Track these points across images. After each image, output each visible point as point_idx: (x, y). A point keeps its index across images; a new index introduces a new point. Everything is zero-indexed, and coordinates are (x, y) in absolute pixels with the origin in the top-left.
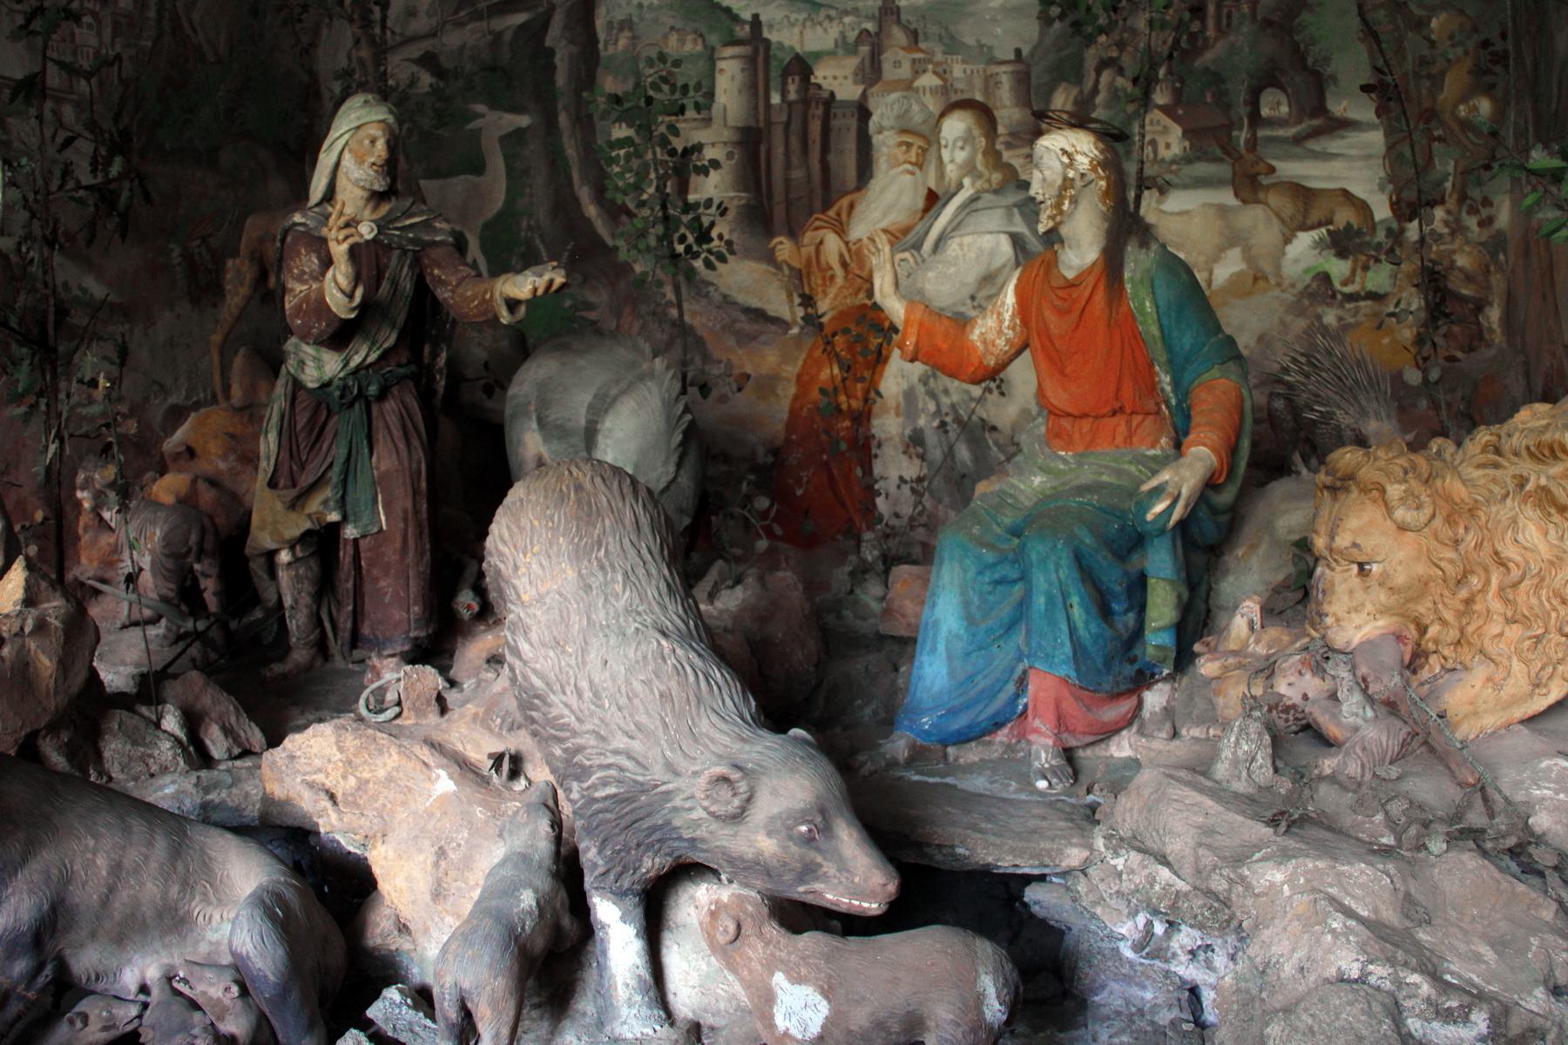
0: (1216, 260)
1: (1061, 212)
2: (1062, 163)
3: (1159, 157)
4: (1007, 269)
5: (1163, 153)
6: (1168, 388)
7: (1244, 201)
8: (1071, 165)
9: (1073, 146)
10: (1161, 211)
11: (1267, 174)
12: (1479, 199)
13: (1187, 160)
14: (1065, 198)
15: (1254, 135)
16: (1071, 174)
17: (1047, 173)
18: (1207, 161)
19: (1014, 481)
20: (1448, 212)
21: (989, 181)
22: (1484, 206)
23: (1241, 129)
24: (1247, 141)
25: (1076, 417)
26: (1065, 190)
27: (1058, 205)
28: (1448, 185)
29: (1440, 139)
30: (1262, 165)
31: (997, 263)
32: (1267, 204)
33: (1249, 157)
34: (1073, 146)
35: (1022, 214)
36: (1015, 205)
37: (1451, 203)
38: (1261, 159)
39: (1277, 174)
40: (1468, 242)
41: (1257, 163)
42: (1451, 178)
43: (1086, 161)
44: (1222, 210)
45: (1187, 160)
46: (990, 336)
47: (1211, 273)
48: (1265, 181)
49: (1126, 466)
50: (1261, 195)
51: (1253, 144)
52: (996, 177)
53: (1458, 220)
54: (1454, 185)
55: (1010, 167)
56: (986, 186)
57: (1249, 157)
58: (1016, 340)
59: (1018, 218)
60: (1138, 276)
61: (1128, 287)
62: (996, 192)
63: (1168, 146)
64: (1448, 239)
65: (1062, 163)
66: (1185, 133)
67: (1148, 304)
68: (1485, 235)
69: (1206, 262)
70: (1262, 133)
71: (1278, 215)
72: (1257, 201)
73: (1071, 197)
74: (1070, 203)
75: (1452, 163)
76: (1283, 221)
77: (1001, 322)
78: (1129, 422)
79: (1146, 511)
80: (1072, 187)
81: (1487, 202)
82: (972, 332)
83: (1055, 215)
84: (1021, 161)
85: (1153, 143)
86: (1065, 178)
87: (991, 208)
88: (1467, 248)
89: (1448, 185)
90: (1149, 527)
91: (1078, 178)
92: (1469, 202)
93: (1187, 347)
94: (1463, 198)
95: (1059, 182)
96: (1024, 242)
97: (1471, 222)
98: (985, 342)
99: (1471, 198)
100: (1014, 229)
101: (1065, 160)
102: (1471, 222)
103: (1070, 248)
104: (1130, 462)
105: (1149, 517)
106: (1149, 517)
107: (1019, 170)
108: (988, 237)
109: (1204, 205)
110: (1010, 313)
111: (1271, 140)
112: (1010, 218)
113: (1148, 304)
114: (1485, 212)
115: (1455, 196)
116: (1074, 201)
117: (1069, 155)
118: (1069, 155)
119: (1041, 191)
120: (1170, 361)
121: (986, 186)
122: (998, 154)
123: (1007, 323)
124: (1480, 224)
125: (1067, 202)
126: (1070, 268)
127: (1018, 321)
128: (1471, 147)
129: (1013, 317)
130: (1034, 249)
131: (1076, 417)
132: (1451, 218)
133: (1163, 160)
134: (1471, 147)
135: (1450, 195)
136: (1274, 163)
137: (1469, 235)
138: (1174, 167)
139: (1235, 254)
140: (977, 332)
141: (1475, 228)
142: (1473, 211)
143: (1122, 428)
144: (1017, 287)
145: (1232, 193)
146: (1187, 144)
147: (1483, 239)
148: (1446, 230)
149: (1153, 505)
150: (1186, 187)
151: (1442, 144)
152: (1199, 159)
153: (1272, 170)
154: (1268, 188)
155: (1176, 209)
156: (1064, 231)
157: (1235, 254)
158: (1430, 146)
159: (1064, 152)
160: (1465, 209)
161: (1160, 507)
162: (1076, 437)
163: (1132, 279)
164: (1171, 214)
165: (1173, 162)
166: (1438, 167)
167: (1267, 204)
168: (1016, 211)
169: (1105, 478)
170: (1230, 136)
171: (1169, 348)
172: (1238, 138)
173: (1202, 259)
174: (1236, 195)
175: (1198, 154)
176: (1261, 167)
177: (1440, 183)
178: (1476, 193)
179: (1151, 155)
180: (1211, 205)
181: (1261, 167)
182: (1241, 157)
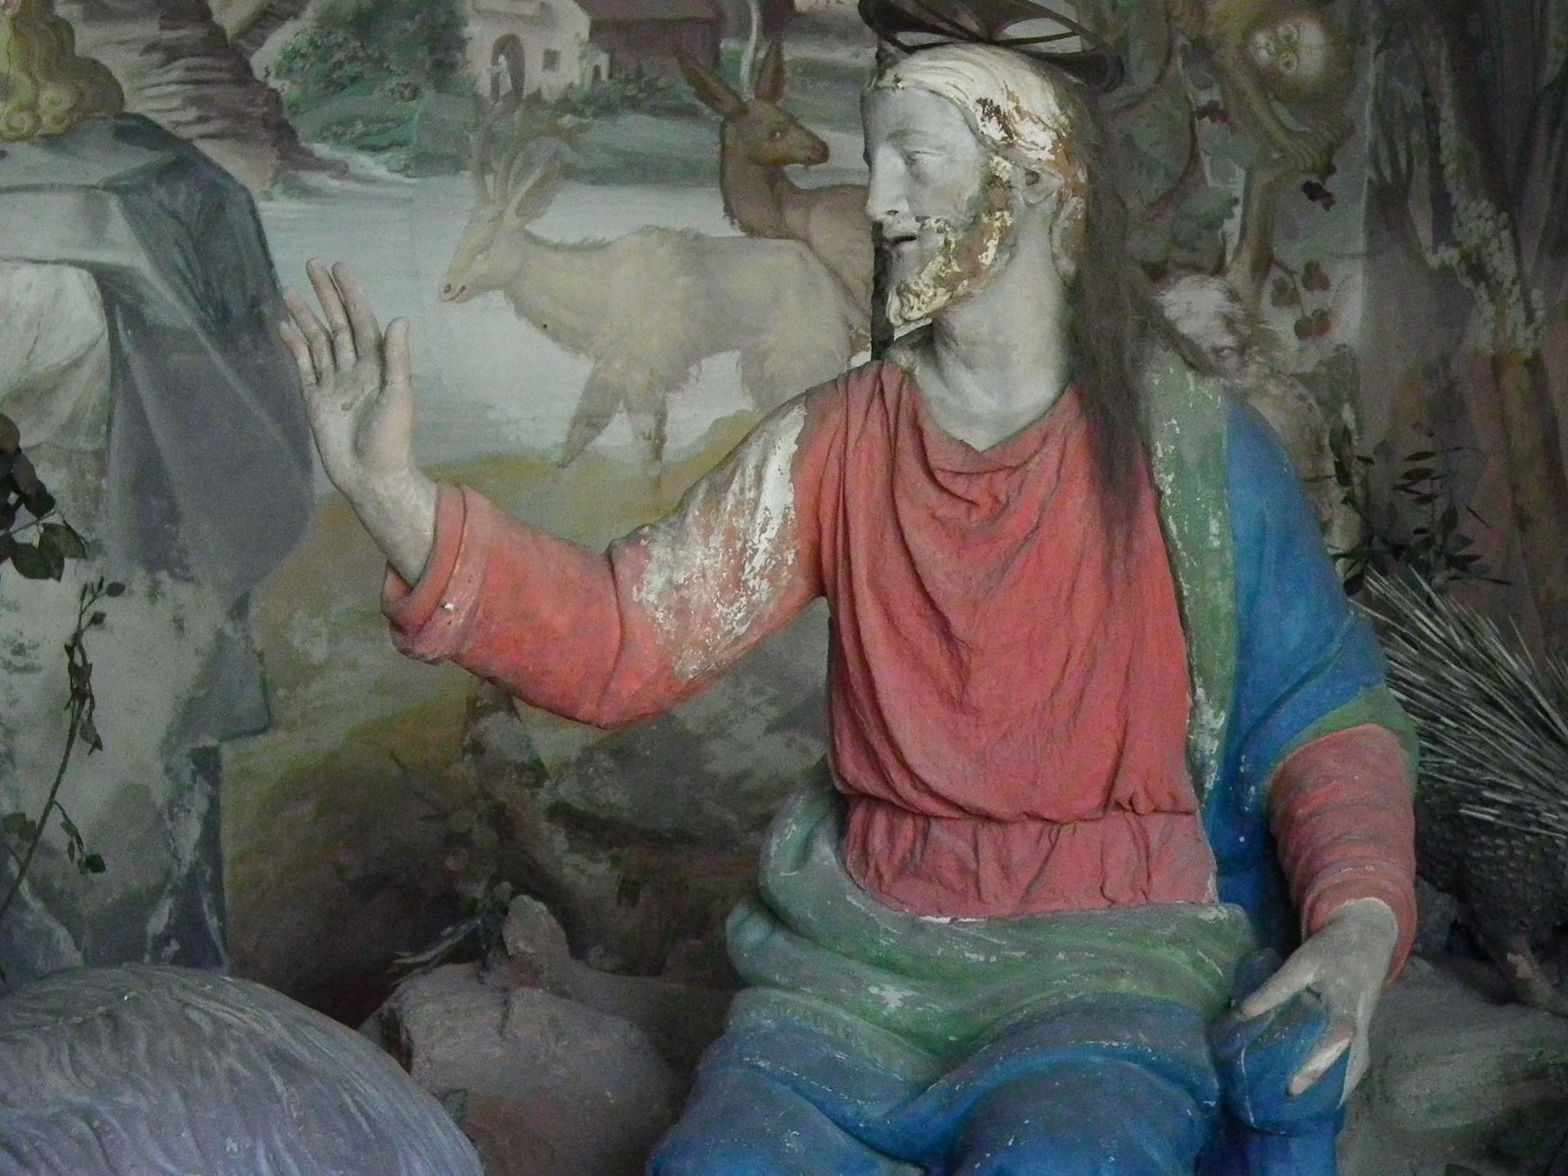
0: (674, 382)
1: (975, 272)
2: (981, 139)
3: (528, 90)
4: (86, 371)
5: (537, 77)
6: (1210, 746)
7: (750, 231)
8: (1008, 145)
9: (1010, 96)
10: (529, 236)
11: (808, 162)
12: (1298, 265)
13: (599, 104)
14: (985, 233)
15: (777, 53)
16: (1004, 168)
17: (931, 162)
18: (655, 112)
19: (809, 1000)
20: (1233, 296)
21: (32, 107)
22: (1308, 284)
23: (743, 33)
24: (758, 69)
25: (970, 814)
26: (990, 213)
27: (967, 252)
28: (1232, 226)
29: (1211, 111)
30: (794, 134)
31: (57, 352)
32: (807, 242)
33: (764, 112)
34: (1010, 96)
35: (133, 214)
36: (111, 187)
37: (1239, 272)
38: (792, 120)
39: (833, 163)
40: (1274, 374)
41: (784, 131)
42: (1238, 210)
43: (1045, 138)
44: (695, 249)
45: (599, 104)
46: (701, 595)
47: (661, 418)
48: (802, 178)
49: (1164, 952)
50: (793, 217)
51: (773, 78)
52: (55, 99)
53: (1253, 318)
54: (1244, 230)
55: (95, 71)
56: (25, 122)
57: (764, 112)
58: (771, 606)
59: (118, 226)
60: (1191, 456)
61: (1166, 480)
62: (51, 141)
63: (551, 59)
64: (1232, 361)
65: (981, 139)
66: (596, 29)
67: (1214, 527)
68: (1310, 358)
69: (650, 387)
70: (796, 51)
71: (834, 273)
72: (784, 233)
73: (1005, 231)
74: (1000, 248)
75: (1240, 174)
76: (847, 290)
77: (740, 557)
78: (1141, 838)
79: (1288, 1066)
80: (1008, 207)
81: (1315, 277)
82: (638, 578)
83: (959, 277)
84: (134, 58)
85: (509, 47)
86: (992, 181)
87: (37, 189)
88: (1273, 388)
89: (1232, 226)
90: (1288, 1112)
91: (1020, 180)
92: (1276, 273)
93: (1294, 640)
94: (1264, 264)
95: (973, 188)
96: (141, 298)
97: (1282, 323)
98: (682, 611)
99: (1280, 265)
100: (106, 257)
101: (993, 130)
102: (1282, 323)
103: (969, 365)
104: (1174, 941)
105: (1299, 1084)
106: (1299, 1084)
107: (126, 87)
108: (28, 273)
109: (646, 231)
110: (771, 533)
111: (813, 71)
112: (97, 230)
113: (1214, 527)
114: (1312, 301)
115: (1247, 257)
116: (1009, 242)
117: (1004, 121)
118: (1004, 121)
119: (904, 207)
120: (1241, 678)
121: (25, 122)
122: (63, 30)
123: (759, 560)
124: (1302, 330)
125: (992, 244)
126: (972, 420)
127: (790, 557)
128: (1280, 136)
129: (779, 544)
130: (166, 320)
131: (970, 814)
132: (1238, 311)
133: (537, 97)
134: (1280, 136)
135: (1238, 250)
136: (825, 134)
137: (1279, 355)
138: (567, 120)
139: (723, 368)
140: (656, 581)
141: (1291, 341)
142: (1285, 296)
143: (1123, 850)
144: (797, 462)
145: (721, 205)
146: (603, 60)
147: (1308, 368)
148: (1228, 341)
149: (1307, 1054)
150: (600, 177)
151: (1217, 125)
152: (634, 105)
153: (822, 153)
154: (813, 196)
155: (573, 238)
156: (963, 322)
157: (723, 368)
158: (1192, 126)
159: (990, 110)
160: (1268, 289)
161: (1323, 1059)
162: (990, 874)
163: (1178, 462)
164: (557, 248)
165: (566, 104)
166: (1211, 183)
167: (807, 242)
168: (113, 203)
169: (1124, 985)
170: (716, 54)
171: (1246, 647)
172: (739, 54)
173: (640, 378)
174: (729, 211)
175: (631, 90)
176: (792, 143)
177: (1212, 224)
178: (1293, 254)
179: (507, 83)
180: (665, 233)
181: (792, 143)
182: (743, 110)
